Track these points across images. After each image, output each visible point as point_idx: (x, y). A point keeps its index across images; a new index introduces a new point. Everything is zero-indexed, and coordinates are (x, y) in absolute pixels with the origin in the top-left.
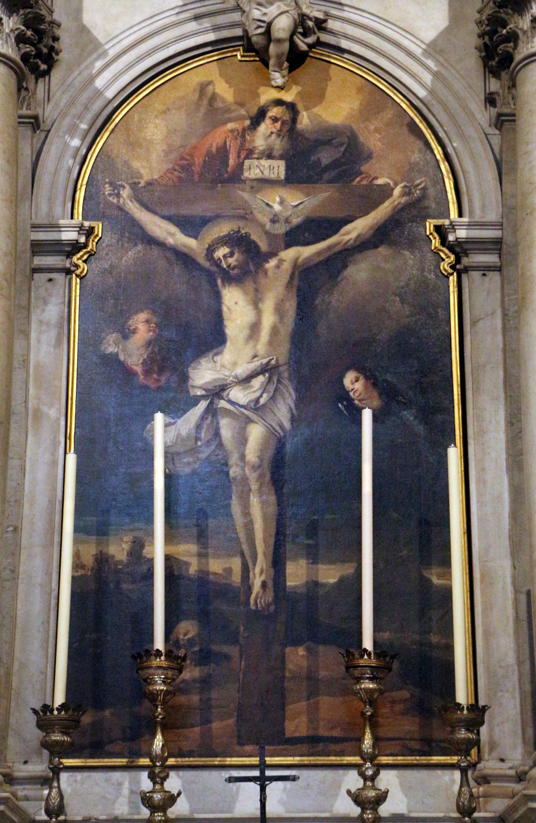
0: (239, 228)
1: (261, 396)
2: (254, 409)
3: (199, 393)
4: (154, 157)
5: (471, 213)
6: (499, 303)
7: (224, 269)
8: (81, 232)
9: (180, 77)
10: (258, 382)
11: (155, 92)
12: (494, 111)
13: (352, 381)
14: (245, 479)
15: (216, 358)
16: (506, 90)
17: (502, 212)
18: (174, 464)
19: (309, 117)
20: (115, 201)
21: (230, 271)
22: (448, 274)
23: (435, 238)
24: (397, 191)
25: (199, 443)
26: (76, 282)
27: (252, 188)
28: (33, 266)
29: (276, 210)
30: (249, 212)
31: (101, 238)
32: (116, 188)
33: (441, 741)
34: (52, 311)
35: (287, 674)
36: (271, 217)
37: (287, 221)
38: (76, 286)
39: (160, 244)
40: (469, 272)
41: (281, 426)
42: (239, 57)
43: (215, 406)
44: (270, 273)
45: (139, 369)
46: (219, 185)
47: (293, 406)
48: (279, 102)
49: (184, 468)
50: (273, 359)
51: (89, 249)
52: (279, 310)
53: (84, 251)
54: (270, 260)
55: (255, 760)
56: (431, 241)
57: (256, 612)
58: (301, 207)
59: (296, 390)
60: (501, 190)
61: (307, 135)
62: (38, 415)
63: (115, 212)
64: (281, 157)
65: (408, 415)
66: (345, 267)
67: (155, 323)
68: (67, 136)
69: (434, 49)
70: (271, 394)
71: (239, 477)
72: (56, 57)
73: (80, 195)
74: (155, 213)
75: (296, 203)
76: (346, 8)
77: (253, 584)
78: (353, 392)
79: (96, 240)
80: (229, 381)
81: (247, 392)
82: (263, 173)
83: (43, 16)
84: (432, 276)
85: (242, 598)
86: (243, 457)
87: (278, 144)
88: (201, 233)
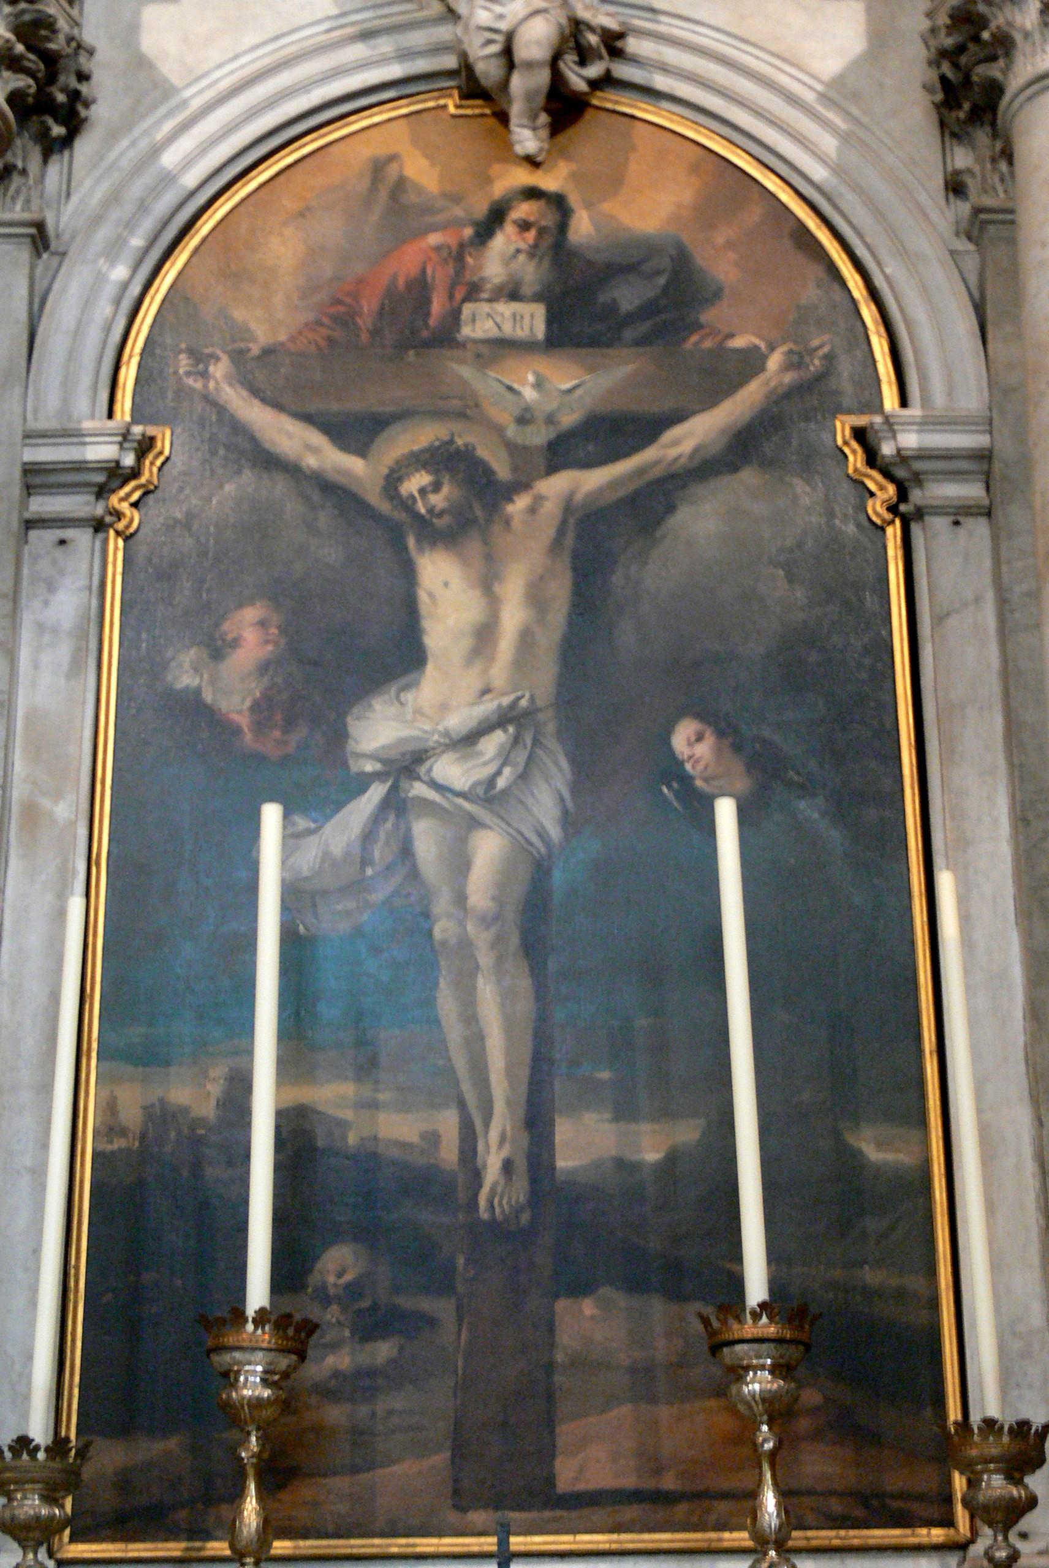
0: (453, 435)
1: (499, 773)
3: (369, 767)
4: (278, 300)
5: (926, 402)
6: (987, 579)
7: (422, 517)
8: (126, 445)
9: (331, 149)
10: (493, 743)
11: (282, 178)
12: (964, 208)
13: (689, 740)
14: (465, 946)
15: (403, 696)
16: (989, 166)
17: (991, 401)
18: (316, 915)
19: (591, 218)
20: (198, 385)
21: (435, 520)
22: (884, 521)
23: (854, 452)
24: (774, 362)
25: (369, 871)
26: (116, 546)
28: (27, 515)
30: (471, 403)
31: (168, 459)
32: (201, 360)
33: (893, 1497)
34: (66, 604)
35: (559, 1357)
36: (517, 412)
37: (550, 420)
38: (115, 554)
40: (927, 518)
41: (542, 834)
42: (452, 109)
43: (403, 795)
44: (516, 523)
45: (244, 721)
46: (412, 352)
47: (567, 795)
48: (533, 193)
49: (332, 922)
50: (523, 696)
51: (143, 480)
52: (536, 598)
53: (132, 484)
54: (515, 498)
55: (489, 1543)
56: (846, 457)
57: (493, 1223)
58: (579, 392)
59: (573, 760)
60: (986, 355)
62: (32, 814)
63: (199, 406)
64: (537, 298)
66: (671, 509)
67: (279, 627)
68: (102, 261)
69: (839, 93)
70: (520, 769)
71: (453, 941)
72: (83, 113)
73: (129, 375)
76: (663, 18)
77: (485, 1166)
78: (692, 761)
79: (159, 463)
80: (431, 744)
81: (469, 764)
82: (500, 328)
83: (50, 16)
84: (851, 528)
85: (462, 1197)
86: (460, 899)
87: (531, 273)
88: (374, 447)
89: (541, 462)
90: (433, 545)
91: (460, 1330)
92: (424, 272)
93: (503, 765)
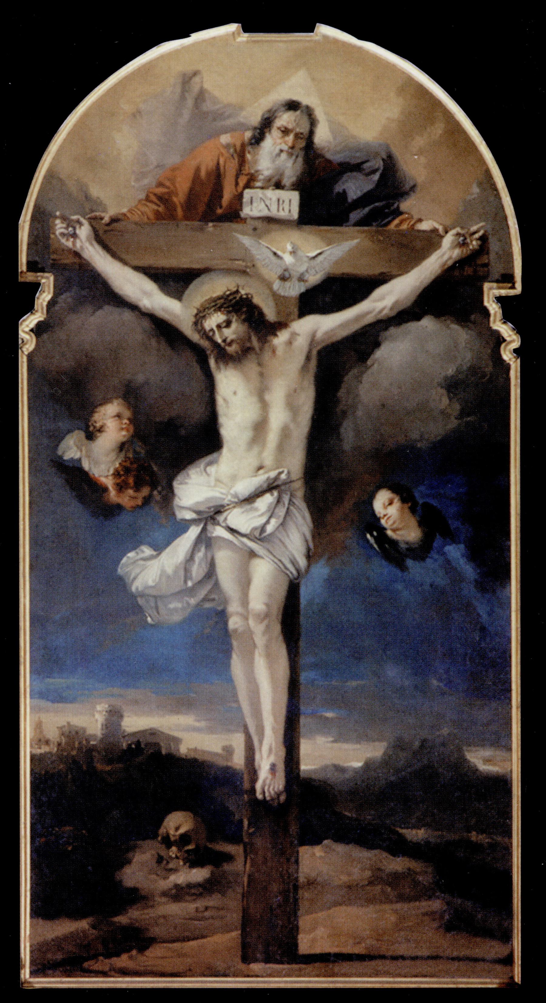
1: (268, 522)
2: (259, 540)
3: (189, 516)
13: (384, 504)
14: (249, 633)
15: (208, 469)
24: (448, 240)
25: (190, 584)
27: (255, 229)
29: (287, 263)
36: (280, 272)
37: (301, 279)
39: (134, 308)
41: (294, 562)
44: (280, 351)
45: (109, 482)
46: (211, 224)
47: (309, 537)
50: (282, 472)
52: (292, 406)
54: (278, 333)
58: (321, 258)
61: (329, 156)
65: (455, 552)
66: (377, 345)
67: (129, 419)
74: (125, 262)
75: (314, 254)
78: (386, 518)
80: (226, 502)
82: (269, 209)
85: (246, 785)
87: (291, 169)
89: (296, 311)
90: (226, 364)
91: (246, 862)
92: (218, 164)
93: (270, 517)
